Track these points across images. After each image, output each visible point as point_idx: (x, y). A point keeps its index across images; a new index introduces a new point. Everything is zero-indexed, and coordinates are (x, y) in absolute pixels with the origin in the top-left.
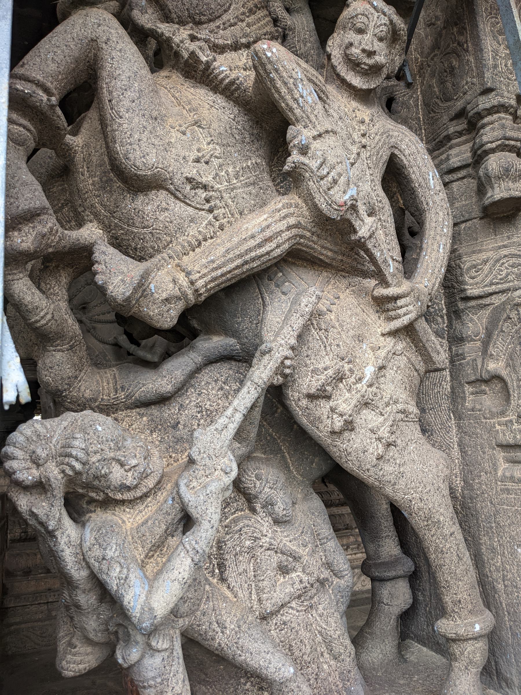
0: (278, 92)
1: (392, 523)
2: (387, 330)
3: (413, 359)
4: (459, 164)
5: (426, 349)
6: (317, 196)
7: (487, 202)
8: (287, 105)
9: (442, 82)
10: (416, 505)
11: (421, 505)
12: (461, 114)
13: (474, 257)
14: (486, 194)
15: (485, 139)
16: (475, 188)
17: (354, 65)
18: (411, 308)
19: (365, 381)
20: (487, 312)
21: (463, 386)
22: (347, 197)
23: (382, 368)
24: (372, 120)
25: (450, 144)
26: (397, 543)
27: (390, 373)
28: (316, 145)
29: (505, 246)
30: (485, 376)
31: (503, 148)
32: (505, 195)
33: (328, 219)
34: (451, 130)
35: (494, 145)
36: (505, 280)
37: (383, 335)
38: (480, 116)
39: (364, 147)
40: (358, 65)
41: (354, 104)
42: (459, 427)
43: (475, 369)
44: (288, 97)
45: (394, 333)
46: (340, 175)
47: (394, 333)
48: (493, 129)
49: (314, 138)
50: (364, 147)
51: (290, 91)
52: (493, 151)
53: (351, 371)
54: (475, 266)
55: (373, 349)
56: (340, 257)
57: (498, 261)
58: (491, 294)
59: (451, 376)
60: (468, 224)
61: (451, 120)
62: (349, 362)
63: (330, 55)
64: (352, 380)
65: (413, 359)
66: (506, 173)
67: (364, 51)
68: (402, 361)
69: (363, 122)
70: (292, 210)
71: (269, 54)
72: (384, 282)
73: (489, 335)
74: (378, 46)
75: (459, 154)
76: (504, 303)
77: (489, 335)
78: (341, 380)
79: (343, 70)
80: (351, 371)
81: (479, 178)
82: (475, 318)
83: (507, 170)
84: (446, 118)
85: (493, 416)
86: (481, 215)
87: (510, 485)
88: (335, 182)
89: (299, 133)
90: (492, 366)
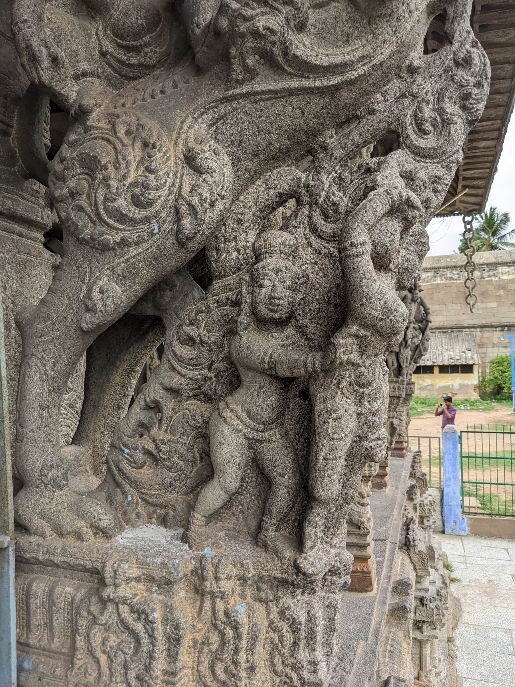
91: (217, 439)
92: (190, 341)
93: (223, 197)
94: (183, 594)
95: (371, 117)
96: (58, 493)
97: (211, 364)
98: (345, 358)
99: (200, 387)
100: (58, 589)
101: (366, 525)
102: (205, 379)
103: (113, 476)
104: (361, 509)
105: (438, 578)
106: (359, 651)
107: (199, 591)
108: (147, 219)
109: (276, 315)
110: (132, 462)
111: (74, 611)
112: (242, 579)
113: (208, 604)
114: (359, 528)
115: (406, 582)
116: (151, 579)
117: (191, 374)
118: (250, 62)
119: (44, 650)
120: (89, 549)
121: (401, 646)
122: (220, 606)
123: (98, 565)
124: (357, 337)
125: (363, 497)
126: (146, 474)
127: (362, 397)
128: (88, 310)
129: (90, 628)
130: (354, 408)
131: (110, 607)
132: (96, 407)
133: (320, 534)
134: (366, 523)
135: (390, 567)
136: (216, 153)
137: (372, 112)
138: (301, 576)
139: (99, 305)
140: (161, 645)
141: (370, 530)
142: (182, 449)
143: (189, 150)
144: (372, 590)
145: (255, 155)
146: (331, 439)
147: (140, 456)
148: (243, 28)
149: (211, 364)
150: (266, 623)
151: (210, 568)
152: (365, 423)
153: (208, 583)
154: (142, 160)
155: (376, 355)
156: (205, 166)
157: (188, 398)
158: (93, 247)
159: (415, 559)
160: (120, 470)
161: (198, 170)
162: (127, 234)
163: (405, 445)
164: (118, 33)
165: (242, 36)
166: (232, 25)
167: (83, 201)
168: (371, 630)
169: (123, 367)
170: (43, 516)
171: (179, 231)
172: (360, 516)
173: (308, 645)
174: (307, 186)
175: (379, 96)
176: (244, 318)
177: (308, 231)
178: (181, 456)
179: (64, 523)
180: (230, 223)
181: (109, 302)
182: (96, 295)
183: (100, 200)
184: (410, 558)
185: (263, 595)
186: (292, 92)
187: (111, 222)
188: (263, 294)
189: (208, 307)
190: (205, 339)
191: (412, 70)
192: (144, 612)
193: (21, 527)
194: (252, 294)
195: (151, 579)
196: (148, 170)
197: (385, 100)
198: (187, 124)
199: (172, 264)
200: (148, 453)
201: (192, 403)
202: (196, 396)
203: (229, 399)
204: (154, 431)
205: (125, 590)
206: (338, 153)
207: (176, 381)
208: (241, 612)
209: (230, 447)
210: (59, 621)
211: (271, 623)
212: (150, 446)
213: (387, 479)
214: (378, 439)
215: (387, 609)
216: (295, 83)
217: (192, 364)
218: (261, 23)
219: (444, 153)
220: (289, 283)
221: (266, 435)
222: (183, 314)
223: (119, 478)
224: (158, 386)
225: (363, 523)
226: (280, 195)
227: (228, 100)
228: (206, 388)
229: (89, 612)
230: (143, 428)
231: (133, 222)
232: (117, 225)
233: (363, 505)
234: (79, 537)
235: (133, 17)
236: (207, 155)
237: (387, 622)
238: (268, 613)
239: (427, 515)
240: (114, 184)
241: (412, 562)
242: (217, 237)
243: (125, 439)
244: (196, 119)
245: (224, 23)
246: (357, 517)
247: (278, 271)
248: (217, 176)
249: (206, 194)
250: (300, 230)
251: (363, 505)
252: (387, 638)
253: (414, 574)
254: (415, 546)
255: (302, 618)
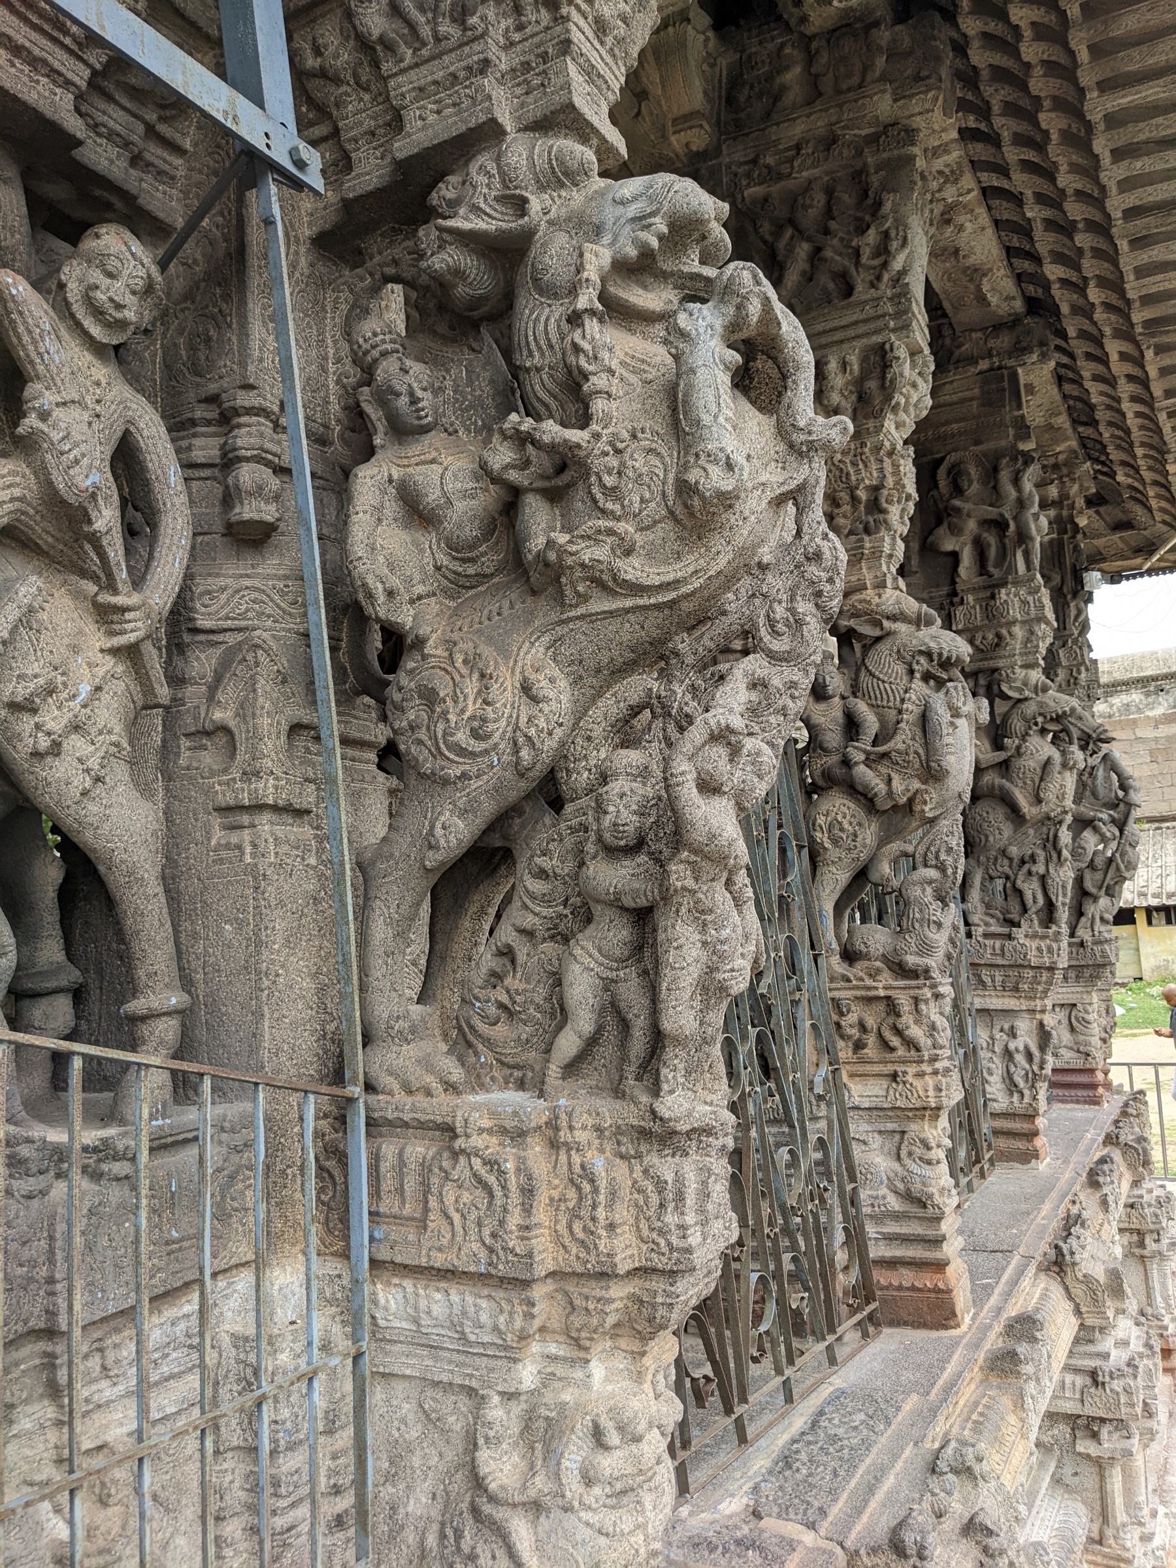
0: (19, 338)
1: (58, 918)
2: (109, 645)
3: (132, 687)
4: (203, 460)
5: (149, 678)
6: (55, 473)
7: (234, 519)
8: (28, 356)
9: (192, 348)
10: (118, 856)
11: (125, 856)
12: (213, 399)
13: (210, 580)
14: (232, 508)
15: (239, 442)
16: (220, 496)
17: (97, 312)
18: (139, 624)
19: (79, 700)
20: (218, 651)
21: (178, 738)
22: (88, 483)
23: (98, 689)
24: (109, 384)
25: (193, 431)
26: (62, 946)
27: (106, 697)
28: (58, 413)
29: (247, 576)
30: (209, 726)
31: (258, 460)
32: (256, 516)
33: (63, 502)
34: (198, 414)
35: (249, 453)
36: (243, 616)
37: (102, 651)
38: (236, 412)
39: (98, 416)
40: (102, 313)
41: (89, 357)
42: (167, 790)
43: (196, 718)
44: (31, 348)
45: (114, 652)
46: (84, 455)
47: (114, 652)
48: (250, 434)
49: (57, 405)
50: (98, 416)
51: (34, 342)
52: (247, 459)
53: (65, 684)
54: (209, 592)
55: (89, 665)
56: (61, 547)
57: (238, 591)
58: (226, 630)
59: (164, 726)
60: (207, 538)
61: (200, 401)
62: (63, 674)
63: (65, 285)
64: (65, 695)
65: (132, 687)
66: (259, 491)
67: (111, 300)
68: (120, 686)
69: (98, 384)
70: (18, 480)
71: (14, 292)
72: (112, 588)
73: (218, 678)
74: (129, 299)
75: (205, 448)
76: (240, 643)
77: (218, 678)
78: (50, 693)
79: (80, 311)
80: (65, 684)
81: (227, 487)
82: (202, 656)
83: (261, 488)
84: (192, 396)
85: (213, 773)
86: (222, 530)
87: (224, 854)
88: (77, 462)
89: (41, 395)
90: (218, 715)
91: (568, 978)
92: (542, 874)
93: (561, 725)
94: (538, 1149)
95: (723, 618)
96: (405, 1047)
97: (567, 899)
98: (679, 884)
99: (556, 927)
100: (409, 1149)
101: (938, 1199)
102: (561, 916)
103: (464, 1036)
104: (927, 1171)
105: (1138, 1337)
106: (907, 1407)
107: (554, 1145)
108: (486, 752)
109: (622, 843)
110: (484, 1018)
111: (425, 1169)
112: (599, 1130)
113: (563, 1158)
114: (925, 1207)
115: (1029, 1317)
116: (503, 1131)
117: (545, 912)
118: (580, 589)
119: (395, 1217)
120: (440, 1105)
121: (1003, 1419)
122: (576, 1159)
123: (449, 1120)
124: (689, 863)
125: (929, 1149)
126: (501, 1031)
127: (705, 925)
128: (431, 847)
129: (442, 1186)
130: (698, 937)
131: (462, 1160)
132: (443, 959)
133: (682, 1080)
134: (936, 1196)
135: (1008, 1295)
136: (552, 681)
137: (724, 613)
138: (658, 1122)
139: (442, 841)
140: (515, 1198)
141: (947, 1210)
142: (539, 1000)
143: (525, 679)
144: (958, 1326)
145: (598, 671)
146: (673, 969)
147: (493, 1010)
148: (569, 561)
149: (567, 899)
150: (630, 1183)
151: (563, 1116)
152: (714, 953)
153: (562, 1133)
154: (479, 692)
155: (713, 880)
156: (541, 695)
157: (544, 940)
158: (435, 781)
159: (1078, 1291)
160: (471, 1027)
161: (535, 700)
162: (467, 767)
163: (1100, 1076)
164: (453, 546)
165: (571, 568)
166: (560, 559)
167: (423, 735)
168: (940, 1382)
169: (473, 909)
170: (390, 1073)
171: (517, 764)
172: (924, 1184)
173: (676, 1208)
174: (659, 697)
175: (730, 596)
176: (590, 848)
177: (663, 745)
178: (538, 1008)
179: (412, 1078)
180: (579, 740)
181: (452, 838)
182: (439, 831)
183: (440, 735)
184: (1067, 1289)
185: (623, 1149)
186: (627, 611)
187: (452, 756)
188: (607, 820)
189: (560, 834)
190: (558, 871)
191: (763, 567)
192: (496, 1162)
193: (369, 1088)
194: (598, 820)
195: (503, 1131)
196: (486, 702)
197: (738, 599)
198: (524, 649)
199: (513, 796)
200: (501, 1006)
201: (548, 946)
202: (552, 937)
203: (580, 936)
204: (508, 981)
205: (477, 1141)
206: (690, 660)
207: (529, 921)
208: (599, 1164)
209: (582, 988)
210: (411, 1184)
211: (635, 1182)
212: (504, 998)
213: (1039, 1142)
214: (732, 970)
215: (981, 1356)
216: (629, 603)
217: (546, 900)
218: (586, 557)
219: (799, 656)
220: (634, 807)
221: (621, 973)
222: (534, 844)
223: (470, 1037)
224: (510, 928)
225: (931, 1196)
226: (631, 707)
227: (563, 622)
228: (562, 927)
229: (441, 1168)
230: (495, 978)
231: (473, 755)
232: (457, 759)
233: (929, 1162)
234: (429, 1093)
235: (467, 529)
236: (543, 684)
237: (982, 1382)
238: (631, 1172)
239: (1152, 1227)
240: (452, 718)
241: (1070, 1298)
242: (566, 757)
243: (476, 991)
244: (532, 644)
245: (552, 556)
246: (919, 1186)
247: (622, 795)
248: (553, 703)
249: (542, 724)
250: (655, 744)
251: (929, 1162)
252: (976, 1404)
253: (1074, 1322)
254: (1074, 1264)
255: (669, 1177)
